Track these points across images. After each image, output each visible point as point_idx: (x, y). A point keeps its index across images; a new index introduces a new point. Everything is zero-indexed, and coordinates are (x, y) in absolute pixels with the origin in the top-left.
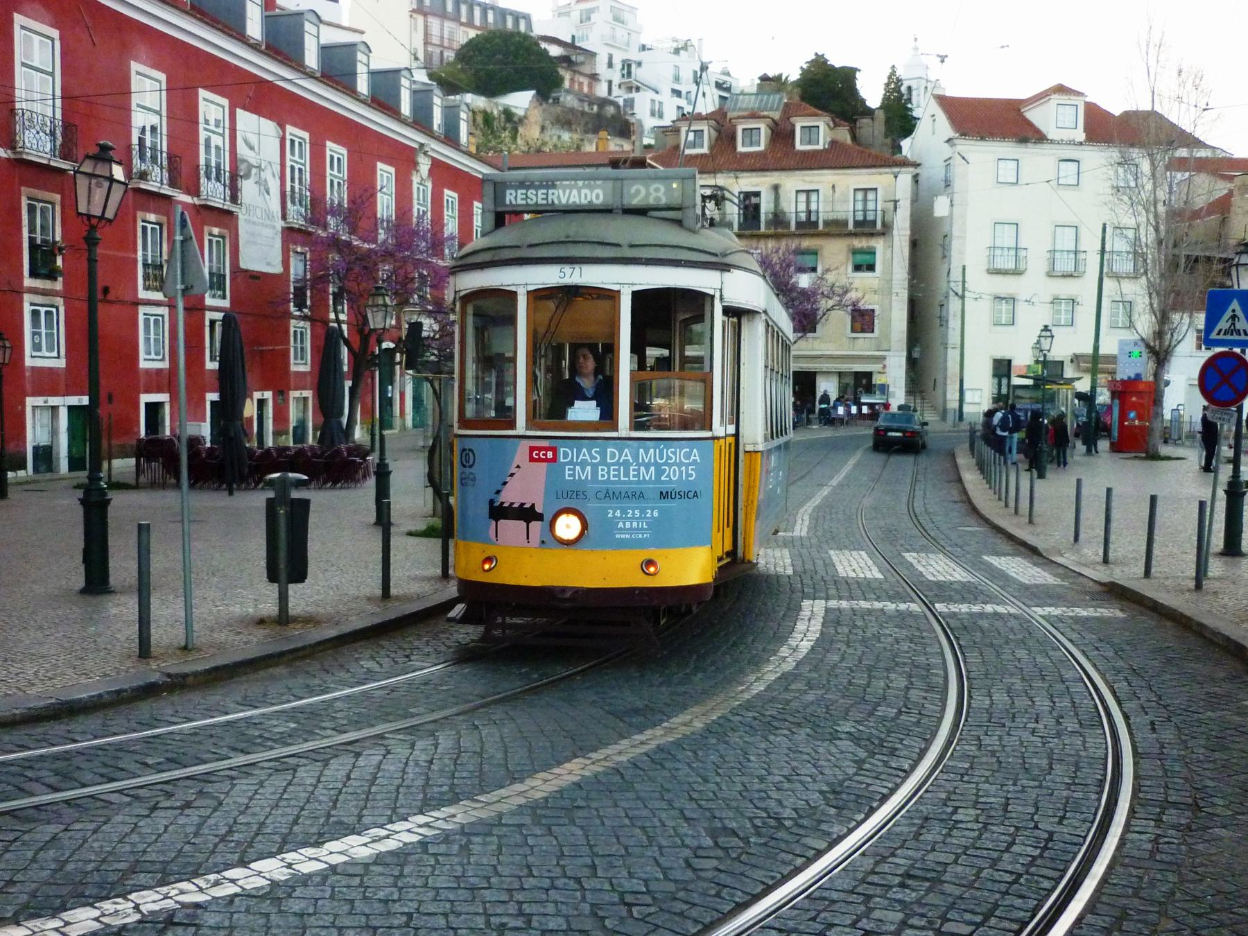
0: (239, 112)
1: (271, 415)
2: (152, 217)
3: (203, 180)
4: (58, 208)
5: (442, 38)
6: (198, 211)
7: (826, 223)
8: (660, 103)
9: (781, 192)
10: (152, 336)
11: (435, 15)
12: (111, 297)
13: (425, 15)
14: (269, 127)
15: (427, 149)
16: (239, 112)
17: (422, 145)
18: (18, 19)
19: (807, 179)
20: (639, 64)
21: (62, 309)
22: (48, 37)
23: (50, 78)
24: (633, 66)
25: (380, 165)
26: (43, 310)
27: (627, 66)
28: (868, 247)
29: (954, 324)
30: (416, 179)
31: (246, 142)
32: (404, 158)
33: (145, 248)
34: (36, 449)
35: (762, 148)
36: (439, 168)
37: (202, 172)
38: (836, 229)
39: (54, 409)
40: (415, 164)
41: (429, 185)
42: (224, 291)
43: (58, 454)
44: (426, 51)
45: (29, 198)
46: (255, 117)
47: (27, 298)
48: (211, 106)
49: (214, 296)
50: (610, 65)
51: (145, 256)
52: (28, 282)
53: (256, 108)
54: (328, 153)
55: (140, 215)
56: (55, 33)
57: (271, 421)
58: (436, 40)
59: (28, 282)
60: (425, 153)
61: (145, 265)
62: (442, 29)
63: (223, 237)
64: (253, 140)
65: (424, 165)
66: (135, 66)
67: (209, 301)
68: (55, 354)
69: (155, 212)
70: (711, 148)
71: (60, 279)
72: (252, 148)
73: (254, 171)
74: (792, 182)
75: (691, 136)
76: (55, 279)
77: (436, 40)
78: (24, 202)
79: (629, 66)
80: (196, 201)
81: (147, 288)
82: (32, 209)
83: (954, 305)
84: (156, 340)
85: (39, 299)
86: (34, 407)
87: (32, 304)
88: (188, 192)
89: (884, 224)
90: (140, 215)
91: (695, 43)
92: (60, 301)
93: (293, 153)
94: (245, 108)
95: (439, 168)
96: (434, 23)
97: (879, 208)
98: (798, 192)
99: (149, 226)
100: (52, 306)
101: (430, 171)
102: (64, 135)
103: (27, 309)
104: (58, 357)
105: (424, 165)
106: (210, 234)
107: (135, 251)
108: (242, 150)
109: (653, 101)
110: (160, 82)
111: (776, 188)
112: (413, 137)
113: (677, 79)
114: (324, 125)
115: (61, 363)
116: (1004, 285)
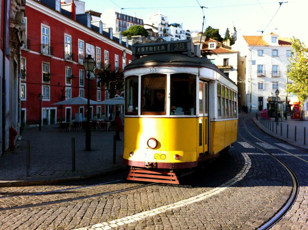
0: (86, 43)
1: (93, 111)
2: (68, 67)
3: (79, 59)
4: (49, 65)
5: (123, 25)
6: (78, 66)
8: (173, 39)
10: (68, 94)
11: (121, 20)
12: (60, 85)
14: (92, 46)
16: (86, 43)
17: (124, 50)
18: (42, 24)
20: (168, 30)
21: (50, 88)
22: (48, 28)
23: (48, 37)
24: (167, 30)
25: (115, 55)
26: (46, 88)
27: (165, 31)
32: (121, 53)
33: (67, 74)
34: (44, 119)
37: (79, 57)
39: (48, 110)
40: (123, 54)
42: (83, 83)
43: (48, 120)
44: (119, 28)
45: (43, 63)
47: (42, 86)
48: (81, 42)
49: (81, 85)
50: (161, 30)
51: (67, 76)
52: (43, 82)
53: (90, 43)
54: (105, 52)
55: (66, 67)
56: (49, 27)
57: (93, 113)
58: (121, 25)
59: (43, 82)
61: (67, 78)
62: (123, 23)
63: (83, 72)
64: (89, 49)
65: (125, 55)
66: (65, 34)
67: (80, 86)
68: (48, 98)
69: (69, 66)
71: (49, 81)
72: (89, 52)
76: (48, 81)
77: (121, 25)
78: (42, 64)
79: (166, 30)
80: (77, 63)
81: (67, 83)
82: (44, 66)
84: (69, 95)
85: (45, 86)
86: (44, 110)
87: (44, 87)
88: (76, 62)
90: (66, 67)
91: (180, 24)
92: (49, 86)
93: (97, 52)
94: (87, 43)
96: (121, 21)
99: (68, 69)
100: (48, 87)
102: (51, 49)
103: (42, 88)
104: (49, 98)
105: (125, 55)
106: (80, 71)
107: (65, 75)
109: (171, 38)
110: (70, 37)
112: (122, 48)
113: (177, 32)
114: (104, 46)
115: (49, 100)
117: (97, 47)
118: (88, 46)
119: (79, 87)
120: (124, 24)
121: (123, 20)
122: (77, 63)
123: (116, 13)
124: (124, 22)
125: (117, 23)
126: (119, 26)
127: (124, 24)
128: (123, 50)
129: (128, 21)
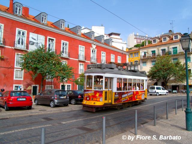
0: (30, 33)
7: (179, 53)
13: (136, 39)
16: (30, 33)
17: (93, 43)
30: (91, 49)
31: (33, 38)
41: (96, 51)
46: (37, 35)
60: (94, 44)
64: (35, 38)
65: (94, 47)
67: (15, 67)
73: (35, 44)
74: (171, 47)
95: (97, 47)
96: (138, 40)
108: (31, 39)
117: (48, 37)
118: (32, 35)
119: (14, 68)
122: (13, 48)
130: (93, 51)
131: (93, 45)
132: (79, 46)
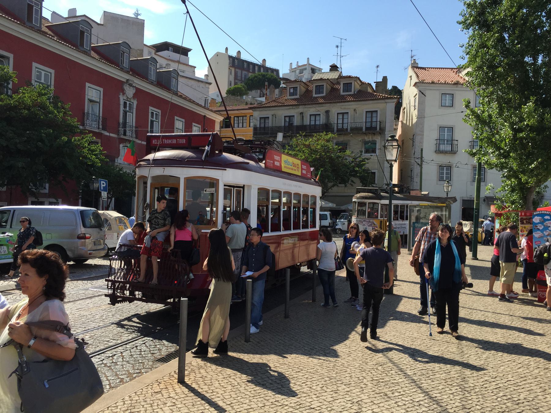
5: (242, 77)
9: (330, 114)
11: (239, 69)
15: (130, 82)
17: (128, 80)
19: (343, 107)
28: (373, 141)
29: (417, 180)
30: (122, 99)
35: (324, 94)
36: (139, 93)
38: (356, 130)
41: (135, 102)
58: (239, 78)
60: (131, 85)
65: (130, 92)
70: (301, 96)
75: (292, 90)
77: (239, 78)
83: (417, 169)
89: (380, 129)
96: (239, 71)
97: (378, 120)
98: (338, 114)
101: (135, 96)
111: (327, 112)
116: (444, 159)
120: (243, 76)
121: (242, 69)
123: (230, 57)
124: (244, 72)
125: (230, 73)
126: (236, 78)
127: (243, 76)
128: (125, 80)
129: (251, 71)
130: (125, 104)
131: (126, 88)
132: (88, 85)
